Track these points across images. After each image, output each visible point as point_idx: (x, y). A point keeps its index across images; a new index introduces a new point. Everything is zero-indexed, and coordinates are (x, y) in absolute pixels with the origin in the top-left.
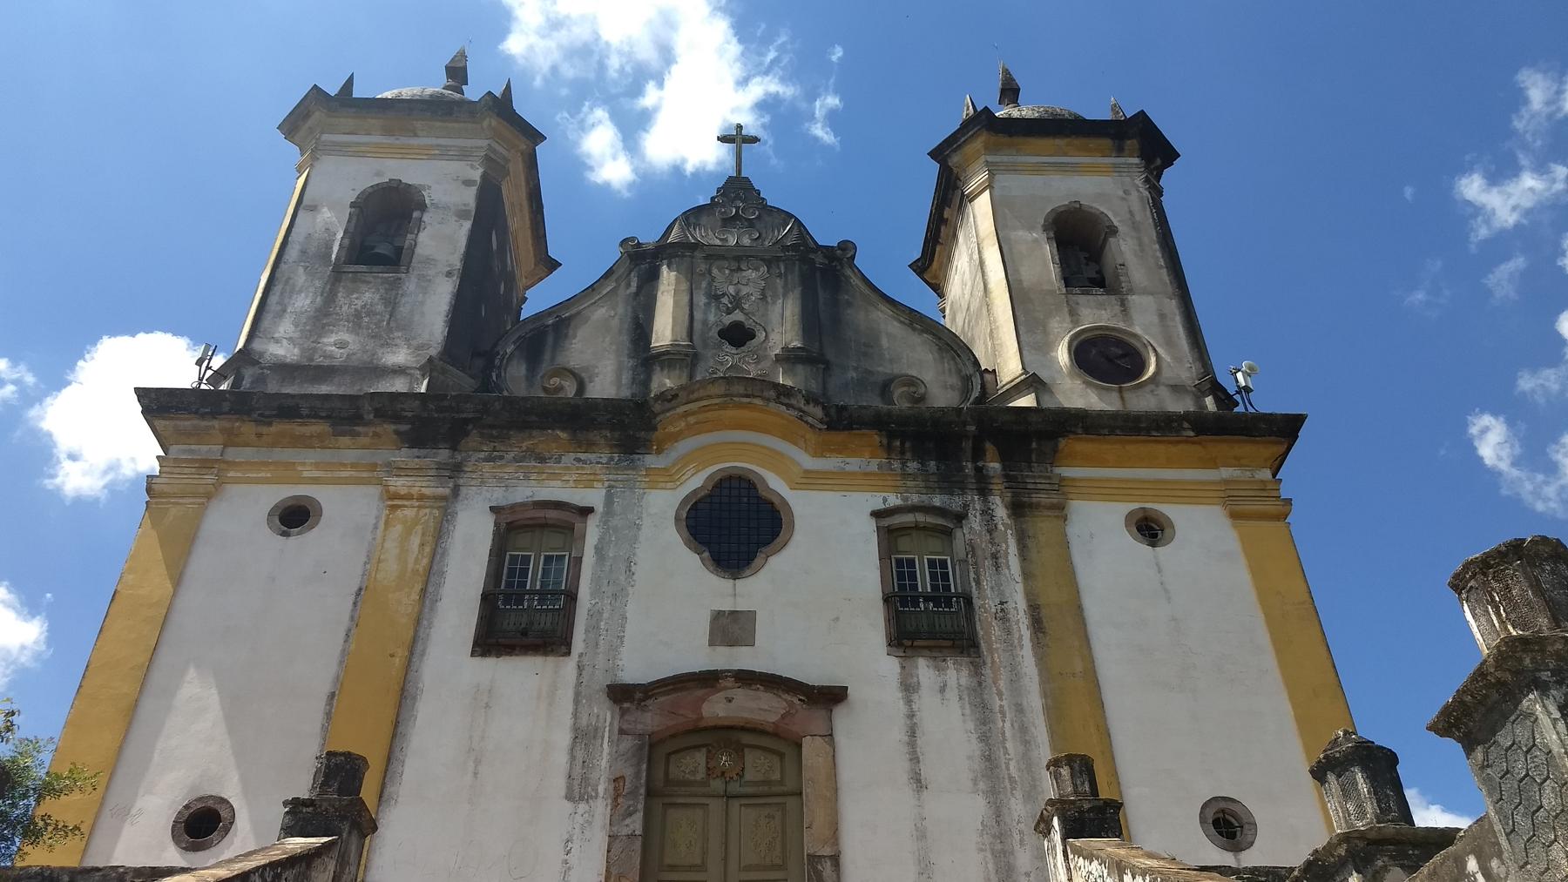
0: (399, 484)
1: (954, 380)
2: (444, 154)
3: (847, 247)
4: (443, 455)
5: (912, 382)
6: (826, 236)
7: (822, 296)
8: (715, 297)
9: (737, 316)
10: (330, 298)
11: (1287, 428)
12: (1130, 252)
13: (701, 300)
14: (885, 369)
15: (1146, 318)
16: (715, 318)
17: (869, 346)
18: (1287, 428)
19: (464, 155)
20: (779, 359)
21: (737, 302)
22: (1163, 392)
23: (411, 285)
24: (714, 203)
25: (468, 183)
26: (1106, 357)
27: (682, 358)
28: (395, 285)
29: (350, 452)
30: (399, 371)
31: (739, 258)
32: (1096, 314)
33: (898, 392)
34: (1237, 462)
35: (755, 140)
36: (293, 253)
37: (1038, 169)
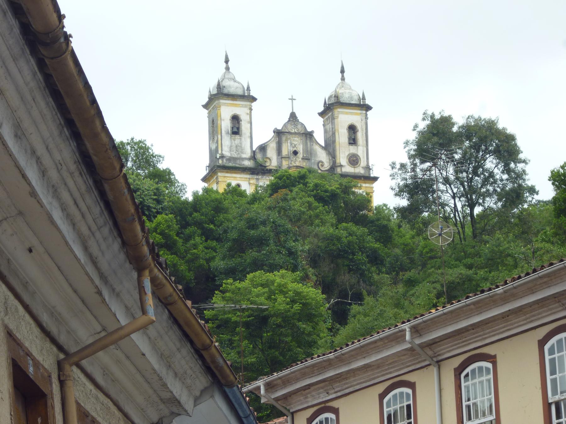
0: (252, 182)
1: (328, 161)
2: (243, 106)
3: (312, 132)
4: (255, 177)
5: (322, 162)
6: (309, 130)
7: (309, 143)
8: (291, 144)
9: (295, 149)
10: (231, 143)
11: (375, 179)
12: (360, 136)
13: (289, 145)
14: (318, 159)
15: (360, 151)
16: (292, 149)
17: (316, 155)
18: (375, 179)
19: (245, 106)
20: (302, 159)
21: (295, 145)
22: (361, 168)
23: (243, 139)
24: (289, 121)
25: (248, 114)
26: (354, 160)
27: (288, 158)
28: (241, 139)
29: (243, 176)
30: (246, 159)
31: (295, 133)
32: (352, 150)
33: (320, 164)
34: (369, 183)
35: (295, 100)
36: (223, 132)
37: (347, 113)
